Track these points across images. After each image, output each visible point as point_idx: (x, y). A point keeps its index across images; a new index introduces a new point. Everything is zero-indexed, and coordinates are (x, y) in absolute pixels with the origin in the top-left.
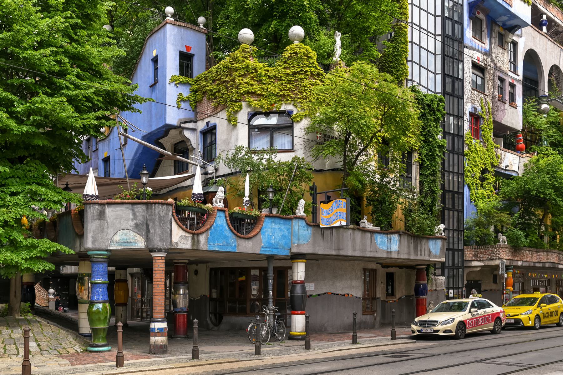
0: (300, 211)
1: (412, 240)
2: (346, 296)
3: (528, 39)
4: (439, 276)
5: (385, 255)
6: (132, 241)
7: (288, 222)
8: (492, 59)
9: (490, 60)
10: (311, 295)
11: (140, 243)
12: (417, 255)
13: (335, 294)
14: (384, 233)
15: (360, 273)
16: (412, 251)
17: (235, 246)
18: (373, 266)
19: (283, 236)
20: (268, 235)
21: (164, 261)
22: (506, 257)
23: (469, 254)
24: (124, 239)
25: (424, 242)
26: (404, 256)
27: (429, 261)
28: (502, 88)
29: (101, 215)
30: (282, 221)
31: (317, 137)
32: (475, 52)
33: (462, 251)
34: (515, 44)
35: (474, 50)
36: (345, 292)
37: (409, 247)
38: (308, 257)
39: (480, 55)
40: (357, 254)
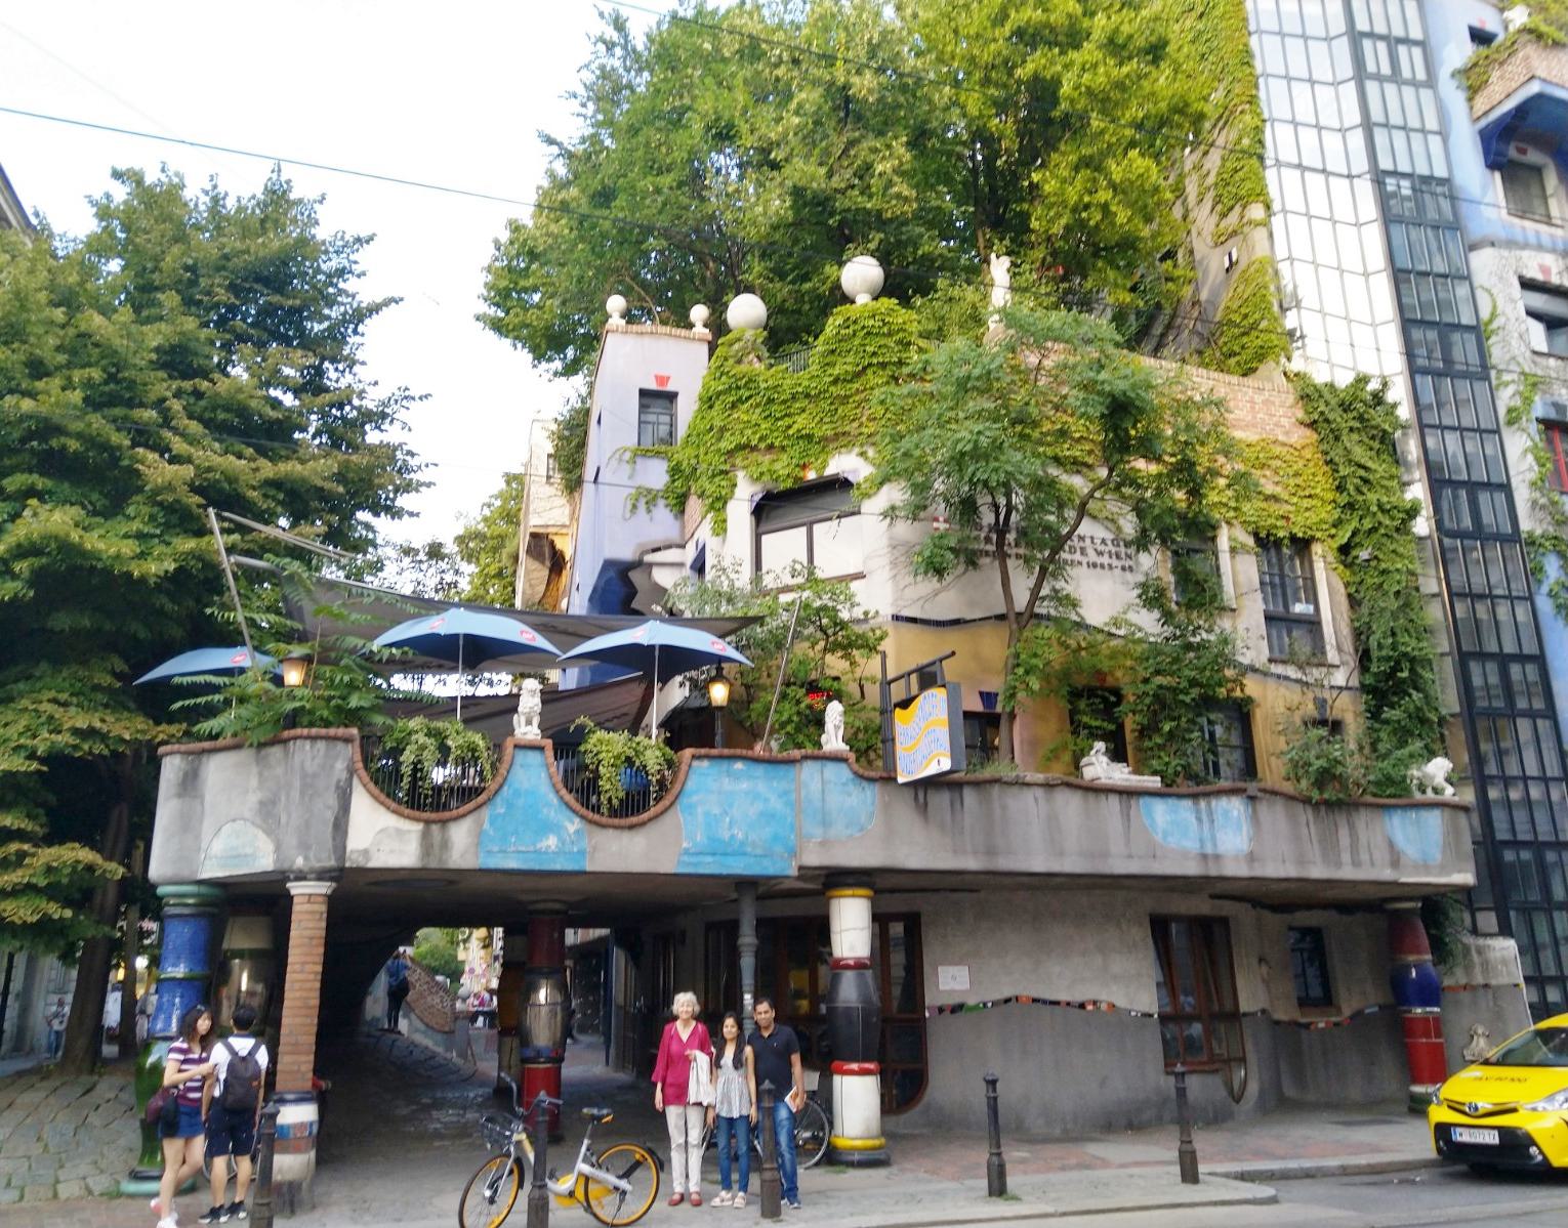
0: (833, 739)
1: (1305, 815)
2: (1090, 1007)
4: (1491, 935)
5: (1192, 869)
7: (782, 770)
10: (957, 1009)
12: (1339, 865)
13: (1045, 1002)
14: (1180, 796)
15: (1142, 935)
16: (1314, 851)
17: (582, 853)
18: (1202, 906)
19: (762, 814)
20: (707, 814)
25: (1362, 818)
27: (1395, 884)
30: (760, 770)
32: (1525, 254)
35: (1525, 246)
38: (880, 882)
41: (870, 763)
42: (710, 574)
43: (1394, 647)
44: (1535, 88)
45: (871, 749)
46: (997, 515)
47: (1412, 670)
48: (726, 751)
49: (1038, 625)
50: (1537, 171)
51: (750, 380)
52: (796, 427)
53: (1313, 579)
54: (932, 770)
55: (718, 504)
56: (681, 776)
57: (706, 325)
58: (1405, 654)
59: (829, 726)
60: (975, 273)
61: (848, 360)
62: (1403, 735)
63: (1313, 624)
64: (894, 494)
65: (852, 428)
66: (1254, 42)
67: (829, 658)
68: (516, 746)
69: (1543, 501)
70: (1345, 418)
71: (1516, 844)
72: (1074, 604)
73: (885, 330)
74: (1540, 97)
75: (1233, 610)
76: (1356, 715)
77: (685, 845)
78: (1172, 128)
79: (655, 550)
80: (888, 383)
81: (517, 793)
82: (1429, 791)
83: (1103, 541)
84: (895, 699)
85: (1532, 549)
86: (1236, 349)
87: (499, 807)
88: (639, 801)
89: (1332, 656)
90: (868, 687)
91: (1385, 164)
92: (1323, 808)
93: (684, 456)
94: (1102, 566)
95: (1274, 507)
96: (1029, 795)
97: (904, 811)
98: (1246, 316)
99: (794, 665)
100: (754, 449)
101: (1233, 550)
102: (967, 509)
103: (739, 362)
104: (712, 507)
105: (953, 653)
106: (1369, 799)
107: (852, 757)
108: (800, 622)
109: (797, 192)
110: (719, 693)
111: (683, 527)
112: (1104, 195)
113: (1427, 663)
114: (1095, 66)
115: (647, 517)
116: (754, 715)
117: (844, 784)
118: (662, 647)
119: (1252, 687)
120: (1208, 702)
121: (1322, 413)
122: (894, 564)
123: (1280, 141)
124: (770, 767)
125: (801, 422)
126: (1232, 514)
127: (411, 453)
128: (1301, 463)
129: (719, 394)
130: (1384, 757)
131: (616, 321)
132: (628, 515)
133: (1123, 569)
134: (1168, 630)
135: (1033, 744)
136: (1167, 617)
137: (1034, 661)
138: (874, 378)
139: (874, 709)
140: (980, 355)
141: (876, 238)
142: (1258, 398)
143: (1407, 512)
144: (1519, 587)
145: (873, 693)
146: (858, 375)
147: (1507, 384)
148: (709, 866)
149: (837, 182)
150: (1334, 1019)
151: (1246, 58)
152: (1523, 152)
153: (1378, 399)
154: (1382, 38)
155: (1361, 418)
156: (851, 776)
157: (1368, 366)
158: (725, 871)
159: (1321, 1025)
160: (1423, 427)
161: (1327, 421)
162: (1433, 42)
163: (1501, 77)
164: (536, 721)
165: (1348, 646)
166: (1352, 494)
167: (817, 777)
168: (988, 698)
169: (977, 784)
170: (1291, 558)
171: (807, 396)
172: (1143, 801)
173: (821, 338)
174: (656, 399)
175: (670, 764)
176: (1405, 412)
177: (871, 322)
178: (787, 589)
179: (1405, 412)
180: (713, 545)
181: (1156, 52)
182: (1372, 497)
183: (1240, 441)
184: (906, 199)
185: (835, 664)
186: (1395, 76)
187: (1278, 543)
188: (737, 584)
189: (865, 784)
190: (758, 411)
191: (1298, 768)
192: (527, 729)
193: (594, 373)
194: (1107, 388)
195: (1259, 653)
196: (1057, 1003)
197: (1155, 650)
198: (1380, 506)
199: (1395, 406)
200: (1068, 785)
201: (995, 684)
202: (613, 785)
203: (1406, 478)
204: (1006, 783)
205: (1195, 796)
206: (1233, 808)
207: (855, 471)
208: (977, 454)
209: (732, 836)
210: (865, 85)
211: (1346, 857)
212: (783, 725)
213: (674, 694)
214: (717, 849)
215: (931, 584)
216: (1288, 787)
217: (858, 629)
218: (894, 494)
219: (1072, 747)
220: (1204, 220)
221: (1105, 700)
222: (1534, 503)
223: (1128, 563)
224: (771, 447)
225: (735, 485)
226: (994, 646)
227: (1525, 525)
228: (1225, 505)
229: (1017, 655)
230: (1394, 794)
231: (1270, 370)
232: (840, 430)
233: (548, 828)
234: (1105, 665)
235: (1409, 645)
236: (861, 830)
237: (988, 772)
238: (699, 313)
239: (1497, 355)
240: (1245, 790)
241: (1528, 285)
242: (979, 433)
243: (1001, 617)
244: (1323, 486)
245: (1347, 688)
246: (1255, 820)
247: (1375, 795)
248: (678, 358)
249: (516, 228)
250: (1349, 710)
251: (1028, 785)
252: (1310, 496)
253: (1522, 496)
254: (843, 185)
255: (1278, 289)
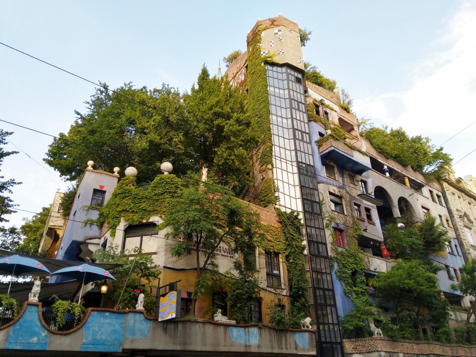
0: (140, 306)
1: (274, 333)
3: (374, 180)
5: (242, 350)
7: (121, 316)
8: (346, 190)
9: (344, 191)
12: (282, 349)
14: (241, 327)
16: (275, 345)
19: (113, 331)
20: (93, 330)
22: (384, 349)
23: (348, 346)
25: (288, 335)
26: (264, 350)
28: (360, 211)
30: (113, 316)
32: (330, 186)
33: (341, 344)
34: (365, 183)
35: (330, 184)
37: (271, 341)
39: (335, 188)
40: (208, 348)
41: (151, 314)
42: (107, 249)
43: (298, 285)
44: (332, 148)
45: (152, 309)
46: (198, 239)
47: (302, 292)
48: (104, 309)
49: (206, 272)
50: (333, 167)
51: (130, 191)
52: (142, 206)
53: (279, 264)
54: (170, 317)
55: (114, 228)
56: (87, 317)
57: (118, 173)
58: (301, 287)
59: (139, 302)
60: (198, 171)
61: (160, 189)
62: (300, 310)
63: (278, 276)
64: (169, 230)
65: (159, 209)
66: (271, 126)
67: (142, 279)
68: (29, 304)
69: (334, 248)
70: (288, 220)
71: (326, 342)
72: (217, 266)
73: (172, 183)
74: (333, 150)
75: (258, 271)
76: (289, 304)
77: (84, 341)
78: (251, 143)
80: (171, 197)
81: (25, 321)
82: (306, 327)
83: (226, 249)
84: (161, 294)
85: (331, 260)
86: (263, 200)
87: (17, 326)
88: (70, 325)
89: (283, 287)
90: (153, 289)
91: (300, 160)
92: (278, 332)
93: (105, 211)
94: (225, 256)
95: (270, 243)
96: (198, 326)
97: (159, 331)
98: (266, 192)
99: (130, 281)
100: (128, 211)
101: (259, 254)
102: (189, 236)
103: (127, 185)
104: (111, 228)
105: (180, 281)
106: (290, 329)
107: (145, 312)
108: (134, 268)
109: (151, 142)
110: (104, 289)
111: (101, 232)
112: (233, 157)
113: (306, 290)
114: (233, 125)
115: (90, 228)
116: (115, 297)
117: (141, 321)
118: (87, 272)
119: (262, 294)
120: (250, 298)
121: (283, 220)
122: (166, 250)
123: (276, 150)
124: (117, 315)
125: (143, 205)
126: (259, 244)
127: (11, 201)
128: (277, 232)
129: (119, 194)
130: (294, 317)
131: (90, 168)
132: (83, 227)
133: (231, 257)
134: (241, 276)
135: (201, 309)
136: (241, 273)
137: (204, 283)
138: (166, 196)
139: (154, 296)
140: (197, 194)
141: (172, 158)
142: (268, 214)
143: (302, 248)
144: (328, 271)
145: (154, 291)
146: (162, 194)
147: (326, 217)
148: (92, 349)
149: (162, 141)
151: (269, 129)
152: (330, 162)
153: (296, 217)
154: (300, 131)
155: (292, 222)
156: (144, 318)
157: (294, 208)
158: (97, 350)
160: (307, 226)
161: (284, 222)
162: (311, 133)
163: (325, 145)
164: (37, 296)
165: (287, 284)
166: (290, 241)
167: (133, 318)
168: (189, 294)
169: (183, 322)
170: (274, 258)
171: (146, 198)
172: (231, 328)
173: (153, 182)
174: (99, 192)
175: (83, 312)
176: (302, 222)
177: (168, 180)
178: (132, 256)
179: (302, 222)
180: (110, 239)
181: (248, 124)
182: (294, 243)
183: (263, 224)
184: (181, 149)
185: (144, 281)
186: (302, 140)
187: (271, 253)
188: (116, 253)
189: (148, 321)
190: (131, 200)
191: (273, 319)
192: (33, 298)
193: (80, 181)
194: (230, 207)
195: (264, 284)
197: (237, 282)
198: (296, 245)
199: (300, 220)
200: (210, 323)
201: (192, 290)
202: (61, 318)
203: (302, 239)
204: (191, 322)
205: (245, 327)
206: (255, 331)
207: (158, 221)
208: (194, 221)
209: (101, 338)
210: (173, 118)
211: (284, 346)
212: (124, 300)
213: (90, 287)
214: (95, 343)
215: (175, 258)
216: (270, 325)
217: (152, 270)
218: (169, 230)
219: (212, 310)
220: (257, 166)
221: (223, 296)
222: (332, 248)
223: (232, 255)
224: (133, 212)
225: (120, 222)
226: (193, 278)
227: (330, 254)
228: (258, 241)
229: (199, 281)
230: (297, 328)
231: (271, 206)
232: (155, 209)
233: (34, 334)
234: (223, 285)
235: (302, 285)
236: (145, 336)
237: (187, 318)
238: (116, 169)
239: (324, 209)
240: (258, 325)
241: (331, 193)
242: (195, 215)
243: (196, 269)
244: (282, 239)
245: (287, 296)
246: (260, 334)
247: (292, 328)
248: (109, 183)
249: (62, 135)
250: (286, 302)
251: (198, 322)
252: (279, 241)
253: (329, 246)
254: (164, 142)
255: (274, 186)
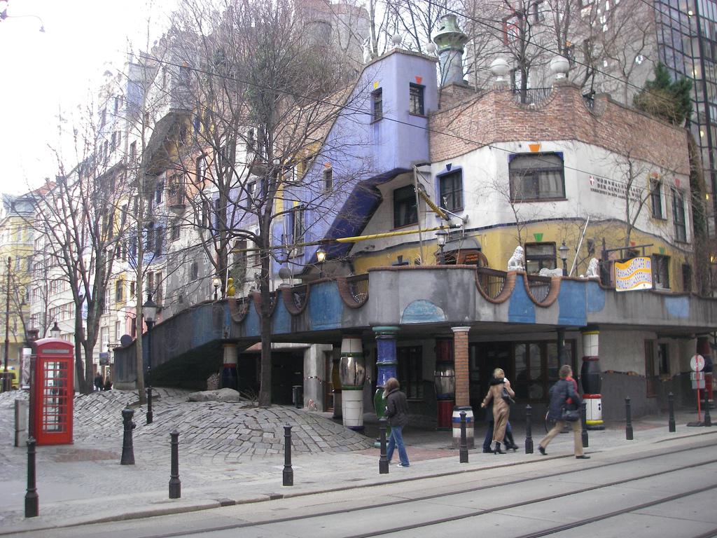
2: (630, 374)
5: (676, 323)
6: (428, 313)
7: (582, 285)
11: (441, 317)
15: (642, 346)
18: (653, 336)
21: (467, 336)
24: (419, 311)
26: (694, 324)
29: (393, 286)
31: (591, 182)
36: (626, 370)
54: (640, 287)
75: (666, 220)
79: (419, 165)
150: (669, 378)
159: (665, 380)
196: (620, 373)
